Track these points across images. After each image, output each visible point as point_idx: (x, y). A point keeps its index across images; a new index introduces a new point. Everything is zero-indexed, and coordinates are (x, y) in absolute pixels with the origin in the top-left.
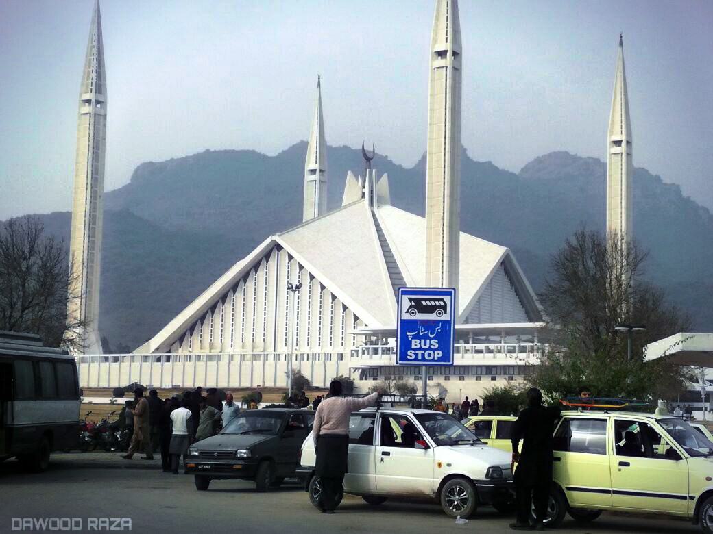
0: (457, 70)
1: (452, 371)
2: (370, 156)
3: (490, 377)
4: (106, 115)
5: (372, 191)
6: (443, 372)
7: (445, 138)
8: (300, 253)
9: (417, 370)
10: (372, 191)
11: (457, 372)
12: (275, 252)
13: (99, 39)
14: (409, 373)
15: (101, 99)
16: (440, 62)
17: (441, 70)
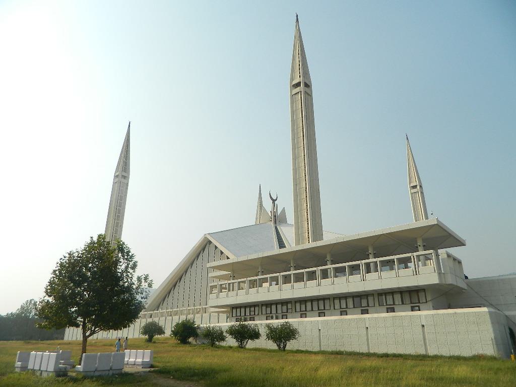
0: (308, 95)
1: (309, 307)
2: (275, 198)
3: (359, 310)
4: (127, 184)
5: (275, 216)
6: (298, 309)
7: (303, 136)
8: (220, 243)
9: (269, 309)
10: (275, 216)
11: (315, 308)
12: (208, 245)
13: (127, 147)
14: (260, 313)
15: (124, 174)
16: (298, 90)
17: (296, 96)
